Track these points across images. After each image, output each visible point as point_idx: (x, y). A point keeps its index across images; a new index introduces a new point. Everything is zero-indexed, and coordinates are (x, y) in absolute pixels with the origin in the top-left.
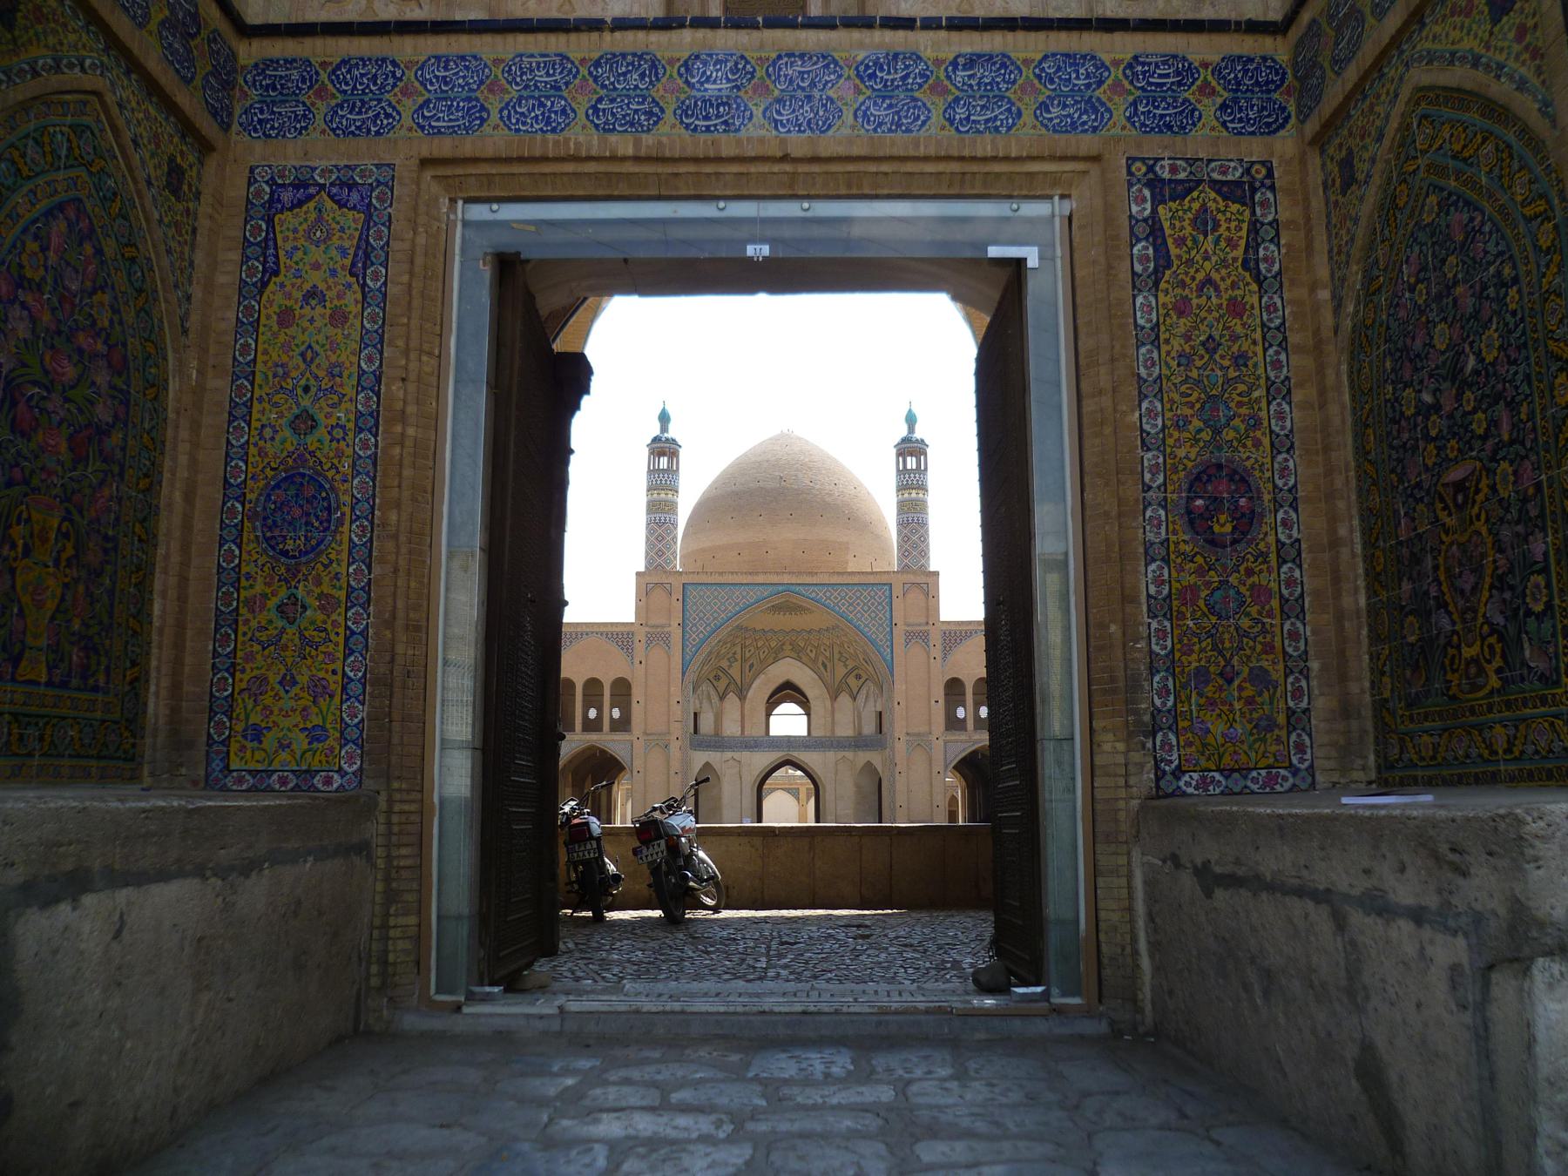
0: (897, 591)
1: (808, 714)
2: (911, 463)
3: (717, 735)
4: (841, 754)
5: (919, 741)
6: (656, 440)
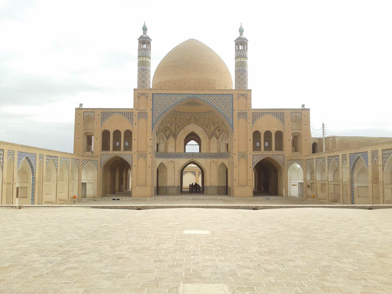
0: (235, 97)
1: (200, 145)
2: (241, 47)
3: (165, 152)
4: (212, 160)
5: (243, 156)
6: (141, 37)
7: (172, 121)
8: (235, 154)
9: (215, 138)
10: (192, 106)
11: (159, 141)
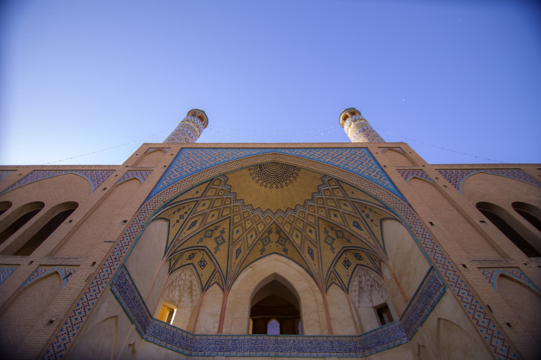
7: (222, 232)
9: (339, 290)
10: (271, 188)
11: (177, 298)
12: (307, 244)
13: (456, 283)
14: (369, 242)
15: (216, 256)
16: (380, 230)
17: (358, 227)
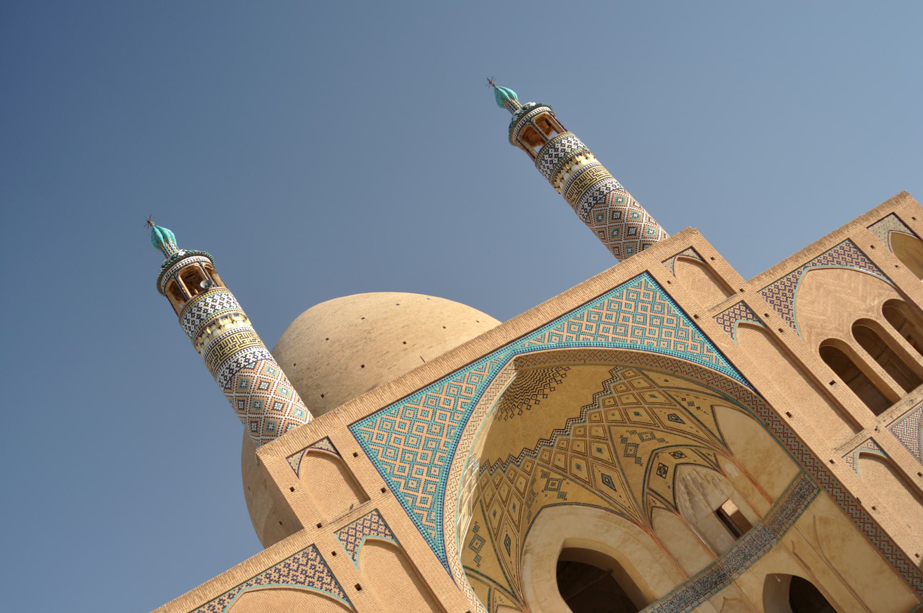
8: (832, 462)
9: (665, 513)
12: (600, 470)
13: (829, 484)
14: (699, 438)
15: (480, 570)
16: (712, 419)
17: (677, 419)
